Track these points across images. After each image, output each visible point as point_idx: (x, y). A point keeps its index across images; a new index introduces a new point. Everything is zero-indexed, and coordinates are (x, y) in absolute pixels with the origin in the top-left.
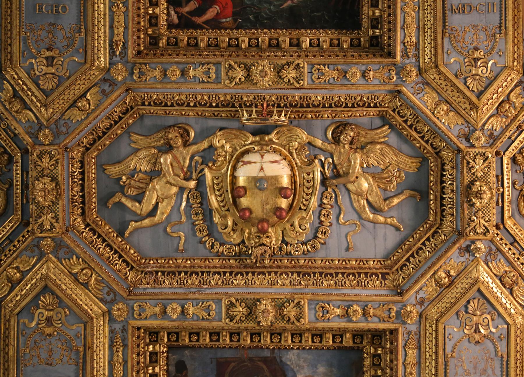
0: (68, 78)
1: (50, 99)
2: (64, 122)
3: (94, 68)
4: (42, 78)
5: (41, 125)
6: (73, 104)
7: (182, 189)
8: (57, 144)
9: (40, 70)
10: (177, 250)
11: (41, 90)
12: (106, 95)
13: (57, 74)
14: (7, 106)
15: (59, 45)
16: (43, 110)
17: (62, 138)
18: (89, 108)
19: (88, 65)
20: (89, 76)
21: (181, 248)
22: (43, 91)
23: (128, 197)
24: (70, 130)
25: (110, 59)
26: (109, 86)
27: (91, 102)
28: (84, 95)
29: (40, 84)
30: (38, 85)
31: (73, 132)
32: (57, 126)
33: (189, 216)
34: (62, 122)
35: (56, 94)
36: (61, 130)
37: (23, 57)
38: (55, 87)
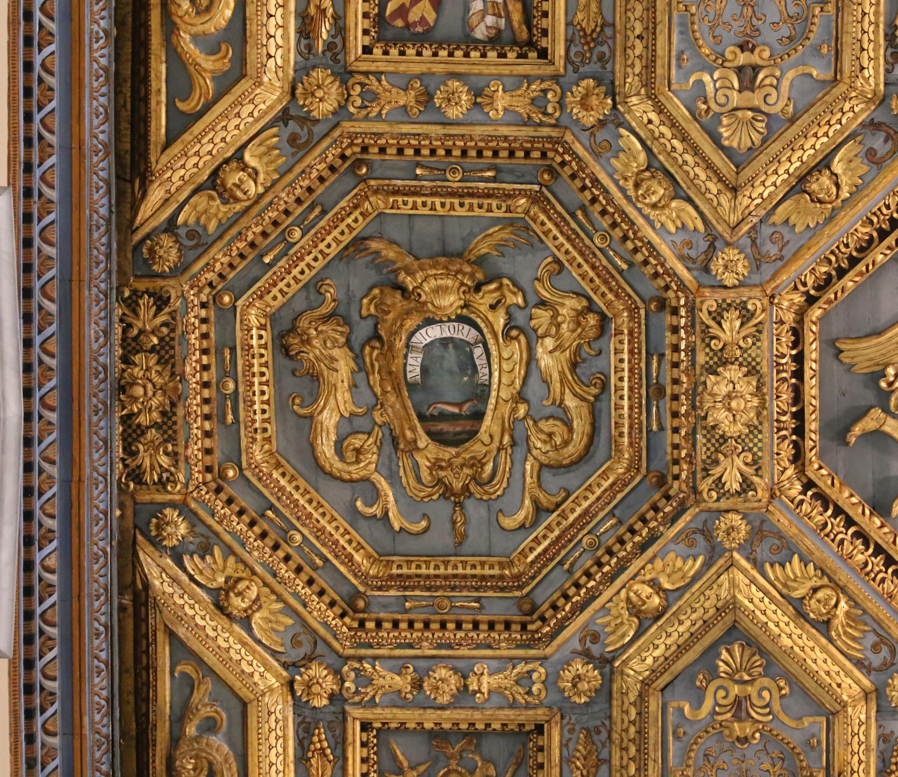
2: (770, 231)
3: (854, 94)
4: (725, 121)
5: (715, 239)
8: (755, 286)
9: (722, 100)
11: (722, 148)
12: (877, 164)
13: (765, 109)
14: (631, 193)
15: (770, 35)
16: (725, 200)
17: (767, 270)
18: (837, 196)
19: (842, 88)
20: (839, 115)
22: (728, 152)
24: (787, 253)
25: (887, 71)
26: (886, 141)
27: (844, 180)
28: (824, 163)
29: (721, 135)
30: (716, 139)
31: (796, 255)
32: (754, 241)
34: (766, 231)
35: (763, 159)
36: (764, 250)
37: (679, 66)
38: (757, 143)
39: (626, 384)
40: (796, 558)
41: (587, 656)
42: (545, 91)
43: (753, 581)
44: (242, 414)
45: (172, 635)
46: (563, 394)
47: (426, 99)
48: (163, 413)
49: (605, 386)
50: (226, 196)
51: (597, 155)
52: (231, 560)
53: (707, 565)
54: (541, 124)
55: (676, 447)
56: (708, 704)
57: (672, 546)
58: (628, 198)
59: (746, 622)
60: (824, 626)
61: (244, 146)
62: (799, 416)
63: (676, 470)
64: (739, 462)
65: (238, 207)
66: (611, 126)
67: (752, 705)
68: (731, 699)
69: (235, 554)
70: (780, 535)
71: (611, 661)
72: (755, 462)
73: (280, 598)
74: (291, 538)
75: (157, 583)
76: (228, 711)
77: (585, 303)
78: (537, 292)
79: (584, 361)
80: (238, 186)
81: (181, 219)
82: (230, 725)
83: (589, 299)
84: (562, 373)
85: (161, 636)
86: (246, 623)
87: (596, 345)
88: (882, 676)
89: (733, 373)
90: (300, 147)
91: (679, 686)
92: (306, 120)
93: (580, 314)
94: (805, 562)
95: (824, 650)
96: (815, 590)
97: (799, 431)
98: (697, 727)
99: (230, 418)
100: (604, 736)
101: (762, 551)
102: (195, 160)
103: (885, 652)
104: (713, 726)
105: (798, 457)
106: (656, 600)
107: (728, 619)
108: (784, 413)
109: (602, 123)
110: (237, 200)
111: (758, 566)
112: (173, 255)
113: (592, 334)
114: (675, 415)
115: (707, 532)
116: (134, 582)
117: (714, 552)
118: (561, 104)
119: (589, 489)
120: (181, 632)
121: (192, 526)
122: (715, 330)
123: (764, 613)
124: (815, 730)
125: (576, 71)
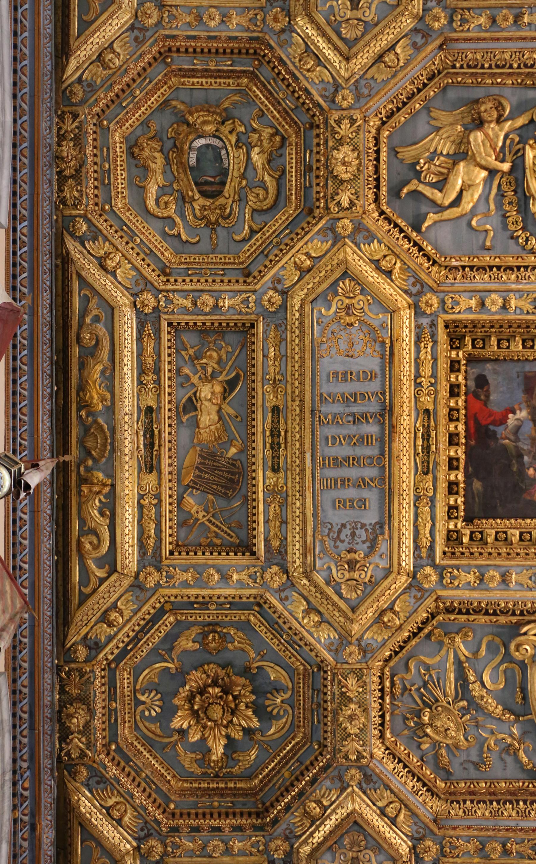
0: (376, 25)
1: (354, 50)
6: (380, 58)
7: (492, 172)
10: (484, 248)
14: (297, 64)
21: (488, 244)
23: (426, 184)
33: (499, 206)
39: (294, 170)
40: (376, 241)
41: (276, 290)
42: (256, 15)
43: (355, 252)
44: (112, 180)
45: (79, 276)
46: (264, 174)
47: (199, 18)
48: (76, 171)
49: (284, 171)
50: (105, 66)
51: (281, 47)
52: (107, 244)
53: (333, 245)
54: (254, 31)
55: (318, 192)
56: (333, 309)
57: (316, 236)
58: (296, 67)
59: (352, 268)
60: (389, 273)
61: (113, 42)
62: (377, 180)
63: (318, 204)
64: (348, 193)
65: (111, 72)
66: (287, 32)
67: (355, 308)
68: (345, 305)
69: (109, 241)
70: (368, 230)
71: (286, 293)
72: (356, 193)
73: (130, 262)
74: (135, 241)
75: (73, 252)
76: (105, 313)
77: (274, 130)
78: (251, 125)
79: (274, 159)
80: (110, 60)
81: (84, 78)
82: (106, 320)
83: (277, 129)
84: (263, 164)
85: (74, 276)
86: (114, 274)
87: (280, 152)
88: (417, 298)
89: (346, 149)
90: (139, 43)
91: (320, 301)
92: (143, 29)
93: (273, 135)
94: (380, 242)
95: (389, 284)
96: (385, 256)
97: (378, 187)
98: (328, 319)
99: (107, 181)
100: (284, 327)
101: (359, 238)
102: (91, 46)
103: (418, 286)
104: (337, 319)
105: (377, 200)
106: (308, 262)
107: (343, 267)
108: (370, 177)
109: (283, 31)
110: (110, 68)
111: (358, 245)
112: (81, 95)
113: (277, 145)
114: (318, 177)
115: (332, 229)
116: (62, 253)
117: (337, 239)
118: (264, 20)
119: (276, 221)
120: (83, 274)
121: (89, 227)
122: (337, 129)
123: (360, 266)
124: (385, 319)
125: (271, 5)
